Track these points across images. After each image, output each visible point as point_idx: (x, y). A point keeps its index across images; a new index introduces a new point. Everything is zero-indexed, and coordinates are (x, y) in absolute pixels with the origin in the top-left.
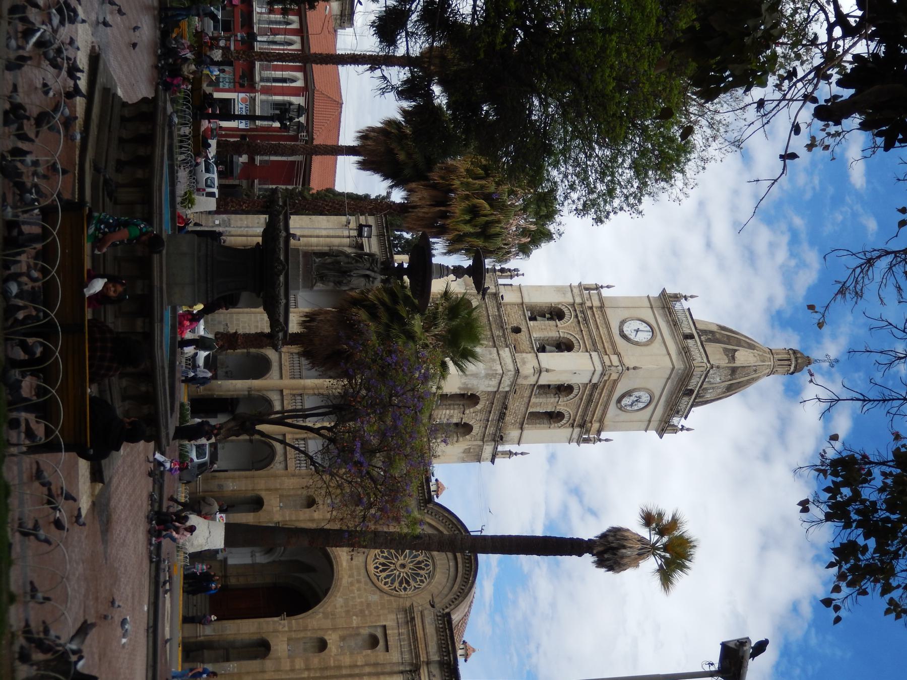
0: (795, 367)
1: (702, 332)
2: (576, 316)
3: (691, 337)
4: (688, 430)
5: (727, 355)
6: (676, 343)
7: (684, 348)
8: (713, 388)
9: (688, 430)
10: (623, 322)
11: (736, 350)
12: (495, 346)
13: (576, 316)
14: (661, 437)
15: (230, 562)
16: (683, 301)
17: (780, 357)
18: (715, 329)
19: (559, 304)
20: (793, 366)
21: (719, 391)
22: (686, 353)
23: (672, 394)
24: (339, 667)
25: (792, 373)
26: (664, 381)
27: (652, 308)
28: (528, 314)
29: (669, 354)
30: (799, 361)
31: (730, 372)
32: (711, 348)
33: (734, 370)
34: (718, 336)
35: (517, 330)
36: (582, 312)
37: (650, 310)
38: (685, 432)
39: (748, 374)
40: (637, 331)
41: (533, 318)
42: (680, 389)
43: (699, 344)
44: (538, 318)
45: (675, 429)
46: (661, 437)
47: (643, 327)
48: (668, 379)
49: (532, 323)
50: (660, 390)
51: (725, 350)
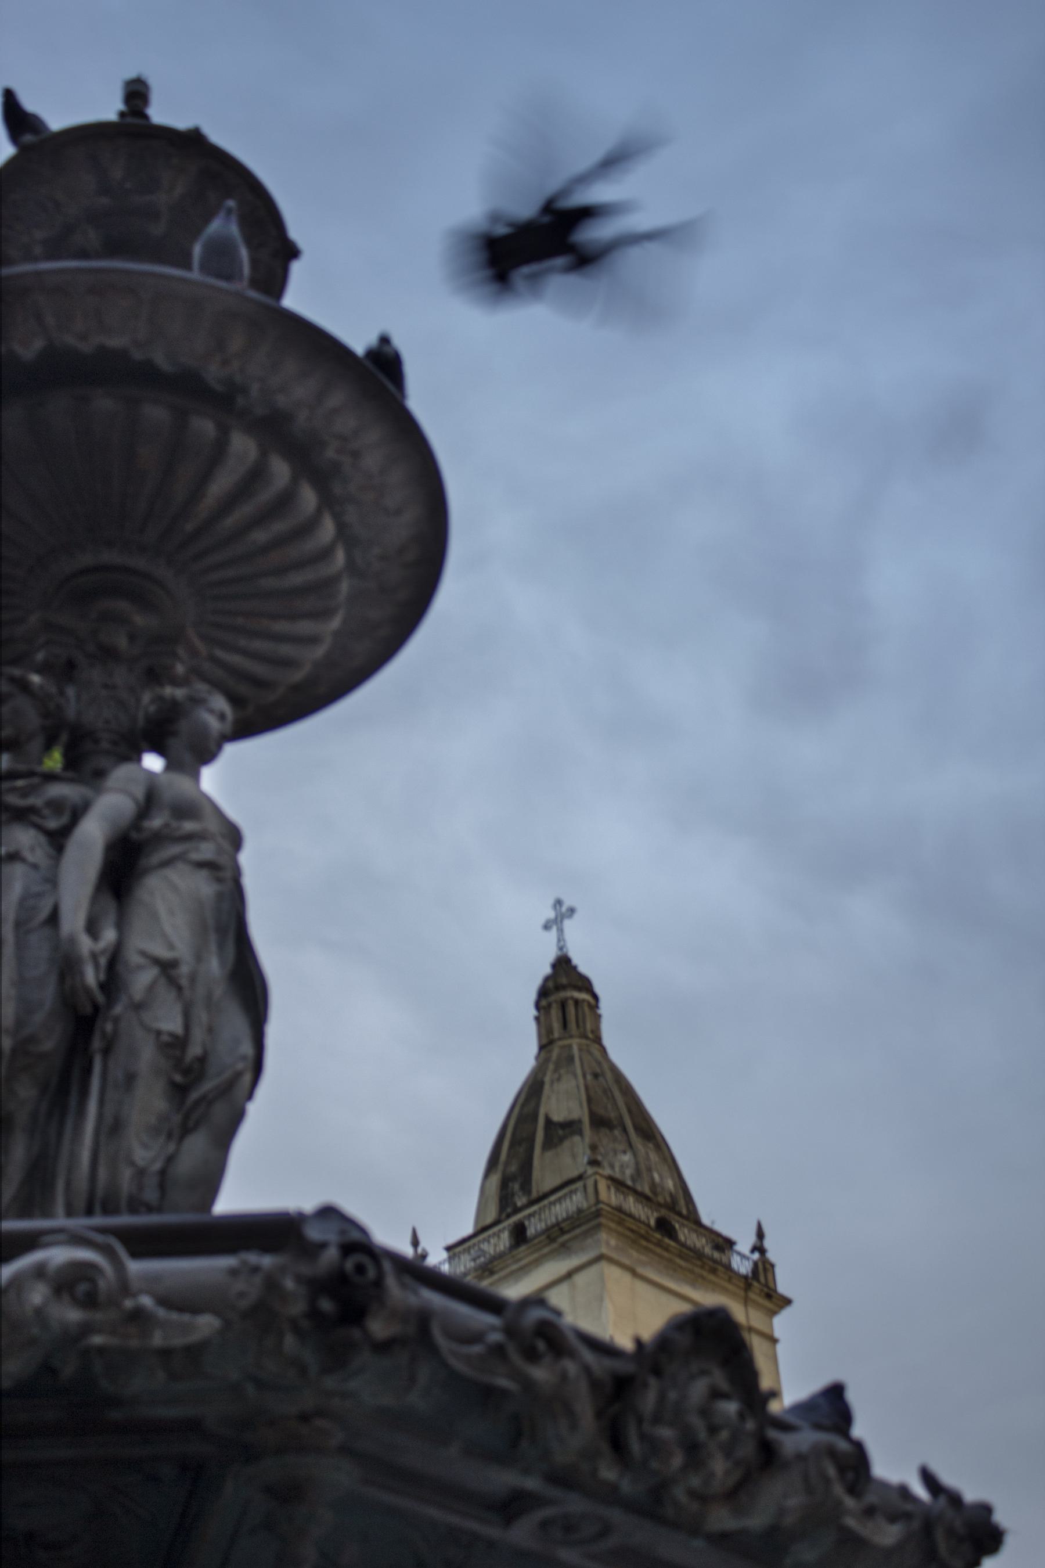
0: (579, 989)
1: (506, 1203)
4: (760, 1235)
5: (561, 1140)
6: (537, 1263)
7: (551, 1240)
8: (649, 1170)
9: (760, 1235)
11: (549, 1122)
14: (787, 1302)
17: (556, 1026)
18: (495, 1179)
20: (577, 995)
21: (654, 1157)
22: (563, 1232)
23: (671, 1268)
25: (596, 997)
26: (641, 1287)
29: (569, 1275)
30: (564, 981)
31: (604, 1131)
32: (544, 1177)
33: (599, 1122)
34: (513, 1168)
38: (767, 1244)
39: (607, 1091)
42: (659, 1244)
43: (535, 1208)
45: (763, 1269)
46: (787, 1302)
48: (634, 1273)
50: (664, 1298)
51: (549, 1143)
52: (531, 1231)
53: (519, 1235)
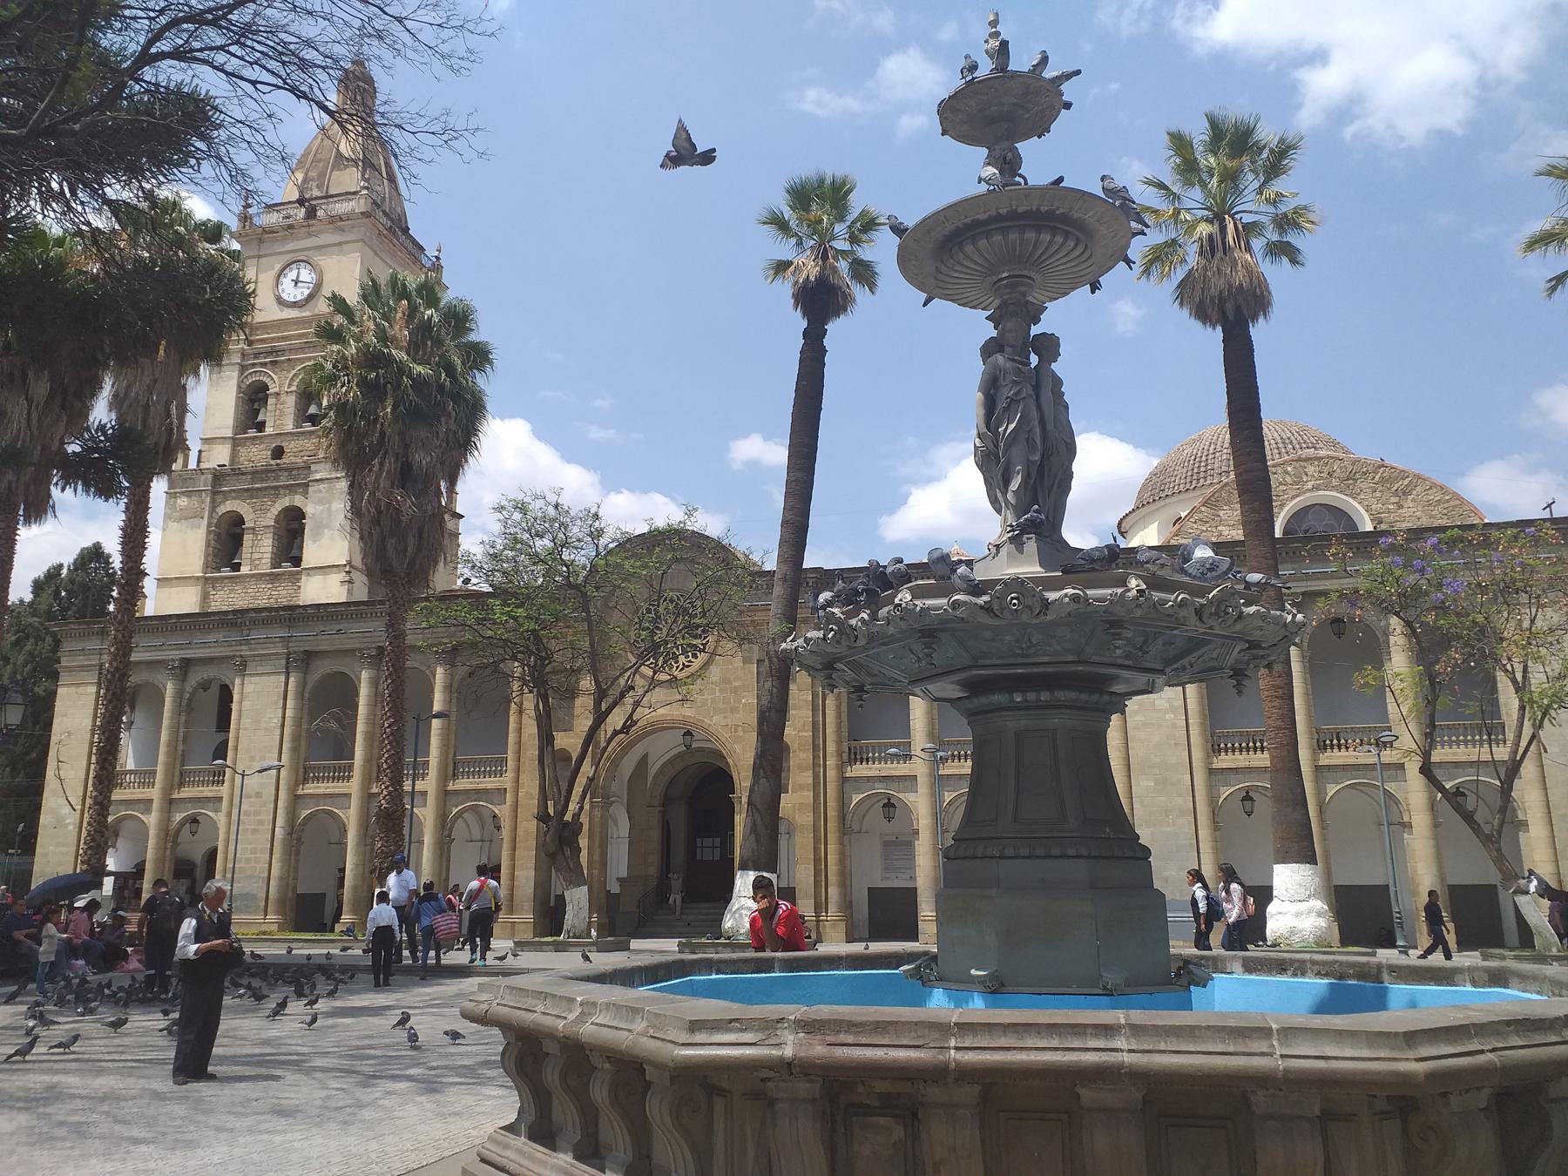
2: (263, 365)
3: (312, 213)
5: (346, 167)
10: (280, 301)
12: (307, 485)
13: (263, 365)
15: (624, 874)
16: (250, 211)
19: (239, 387)
24: (815, 724)
27: (259, 257)
28: (252, 433)
29: (340, 244)
35: (278, 452)
36: (256, 356)
37: (263, 260)
40: (296, 282)
41: (261, 426)
44: (260, 418)
47: (292, 275)
49: (269, 430)
52: (320, 213)
53: (312, 213)
